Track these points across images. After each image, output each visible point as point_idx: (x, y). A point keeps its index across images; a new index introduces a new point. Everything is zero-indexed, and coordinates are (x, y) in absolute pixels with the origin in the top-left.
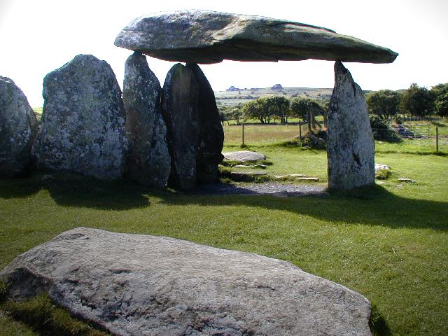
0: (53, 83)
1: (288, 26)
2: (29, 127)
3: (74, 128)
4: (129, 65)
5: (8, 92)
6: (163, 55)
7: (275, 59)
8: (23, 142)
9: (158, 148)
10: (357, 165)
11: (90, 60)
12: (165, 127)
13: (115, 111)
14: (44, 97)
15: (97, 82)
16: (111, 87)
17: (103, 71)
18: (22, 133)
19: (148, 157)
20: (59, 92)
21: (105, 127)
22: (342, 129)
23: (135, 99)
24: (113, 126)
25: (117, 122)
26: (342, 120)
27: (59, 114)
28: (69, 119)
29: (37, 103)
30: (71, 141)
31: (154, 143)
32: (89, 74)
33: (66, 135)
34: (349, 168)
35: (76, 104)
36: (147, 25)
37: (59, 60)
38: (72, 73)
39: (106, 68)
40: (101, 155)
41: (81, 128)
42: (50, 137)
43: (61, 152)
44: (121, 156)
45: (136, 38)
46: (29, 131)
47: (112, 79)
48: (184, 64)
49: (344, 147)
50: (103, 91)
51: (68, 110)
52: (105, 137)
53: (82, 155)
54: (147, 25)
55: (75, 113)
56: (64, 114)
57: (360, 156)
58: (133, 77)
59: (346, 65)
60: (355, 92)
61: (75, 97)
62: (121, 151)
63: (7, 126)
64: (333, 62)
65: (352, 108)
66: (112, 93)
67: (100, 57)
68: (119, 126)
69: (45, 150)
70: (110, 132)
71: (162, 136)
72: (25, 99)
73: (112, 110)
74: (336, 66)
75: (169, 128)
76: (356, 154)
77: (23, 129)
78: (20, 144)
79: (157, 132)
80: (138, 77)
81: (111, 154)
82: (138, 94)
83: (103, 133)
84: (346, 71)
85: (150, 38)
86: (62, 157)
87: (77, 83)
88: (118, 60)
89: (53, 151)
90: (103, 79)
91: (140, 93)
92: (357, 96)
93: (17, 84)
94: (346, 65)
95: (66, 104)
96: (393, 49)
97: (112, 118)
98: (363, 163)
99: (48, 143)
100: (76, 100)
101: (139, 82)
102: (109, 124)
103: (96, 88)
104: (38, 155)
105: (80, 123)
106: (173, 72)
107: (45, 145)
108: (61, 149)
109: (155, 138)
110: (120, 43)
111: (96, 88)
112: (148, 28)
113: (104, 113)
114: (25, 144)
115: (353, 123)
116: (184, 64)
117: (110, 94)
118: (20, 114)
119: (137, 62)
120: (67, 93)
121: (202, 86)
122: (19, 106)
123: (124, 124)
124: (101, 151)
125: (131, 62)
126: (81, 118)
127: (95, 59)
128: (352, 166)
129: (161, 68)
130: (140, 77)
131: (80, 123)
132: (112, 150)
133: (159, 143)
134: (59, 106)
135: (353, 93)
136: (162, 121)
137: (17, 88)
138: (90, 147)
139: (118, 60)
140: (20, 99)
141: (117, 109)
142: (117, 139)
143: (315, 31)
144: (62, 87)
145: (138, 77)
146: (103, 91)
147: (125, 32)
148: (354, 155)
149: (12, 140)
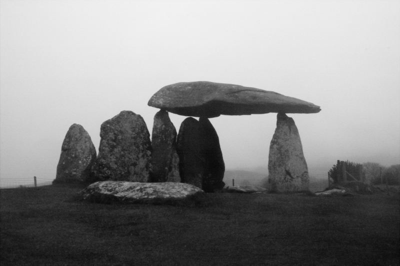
0: (106, 128)
1: (246, 91)
3: (118, 156)
4: (157, 118)
5: (80, 133)
6: (179, 111)
7: (249, 113)
10: (290, 178)
11: (130, 113)
12: (178, 158)
13: (144, 146)
14: (101, 135)
15: (134, 128)
16: (142, 131)
17: (138, 121)
18: (86, 158)
20: (110, 133)
21: (138, 156)
22: (279, 155)
23: (160, 140)
24: (143, 156)
25: (146, 154)
27: (109, 147)
28: (116, 150)
29: (96, 141)
30: (116, 163)
31: (170, 169)
32: (130, 123)
33: (113, 160)
34: (283, 178)
36: (168, 92)
37: (111, 114)
38: (119, 122)
39: (140, 119)
41: (123, 156)
42: (103, 160)
43: (110, 170)
44: (148, 175)
45: (161, 102)
46: (91, 157)
47: (144, 126)
48: (198, 119)
49: (280, 166)
50: (138, 134)
51: (115, 144)
52: (138, 163)
53: (123, 173)
54: (168, 92)
55: (120, 147)
57: (291, 171)
58: (159, 126)
60: (290, 132)
61: (120, 137)
65: (287, 142)
66: (143, 135)
67: (137, 113)
68: (147, 156)
69: (100, 169)
70: (141, 159)
71: (176, 165)
72: (89, 138)
73: (143, 146)
74: (278, 117)
76: (287, 169)
79: (173, 163)
80: (162, 126)
81: (141, 174)
82: (162, 137)
83: (136, 160)
85: (169, 100)
86: (110, 173)
87: (121, 128)
88: (149, 116)
89: (105, 169)
90: (138, 126)
91: (163, 136)
92: (291, 133)
93: (85, 128)
94: (289, 115)
95: (114, 141)
97: (143, 151)
99: (102, 164)
100: (120, 138)
101: (163, 129)
103: (133, 131)
104: (95, 172)
105: (122, 153)
106: (184, 123)
107: (100, 165)
108: (109, 168)
109: (171, 166)
110: (150, 104)
111: (133, 131)
112: (169, 94)
115: (287, 151)
116: (198, 119)
117: (142, 136)
118: (86, 147)
119: (162, 116)
120: (115, 134)
121: (212, 136)
122: (85, 142)
123: (151, 155)
125: (158, 116)
126: (123, 150)
127: (133, 114)
128: (285, 178)
129: (177, 120)
130: (164, 126)
131: (122, 153)
132: (142, 171)
133: (173, 169)
134: (110, 142)
136: (176, 154)
137: (85, 131)
138: (128, 168)
139: (149, 116)
140: (86, 137)
143: (262, 94)
144: (112, 131)
145: (162, 126)
147: (155, 96)
148: (286, 170)
149: (80, 162)
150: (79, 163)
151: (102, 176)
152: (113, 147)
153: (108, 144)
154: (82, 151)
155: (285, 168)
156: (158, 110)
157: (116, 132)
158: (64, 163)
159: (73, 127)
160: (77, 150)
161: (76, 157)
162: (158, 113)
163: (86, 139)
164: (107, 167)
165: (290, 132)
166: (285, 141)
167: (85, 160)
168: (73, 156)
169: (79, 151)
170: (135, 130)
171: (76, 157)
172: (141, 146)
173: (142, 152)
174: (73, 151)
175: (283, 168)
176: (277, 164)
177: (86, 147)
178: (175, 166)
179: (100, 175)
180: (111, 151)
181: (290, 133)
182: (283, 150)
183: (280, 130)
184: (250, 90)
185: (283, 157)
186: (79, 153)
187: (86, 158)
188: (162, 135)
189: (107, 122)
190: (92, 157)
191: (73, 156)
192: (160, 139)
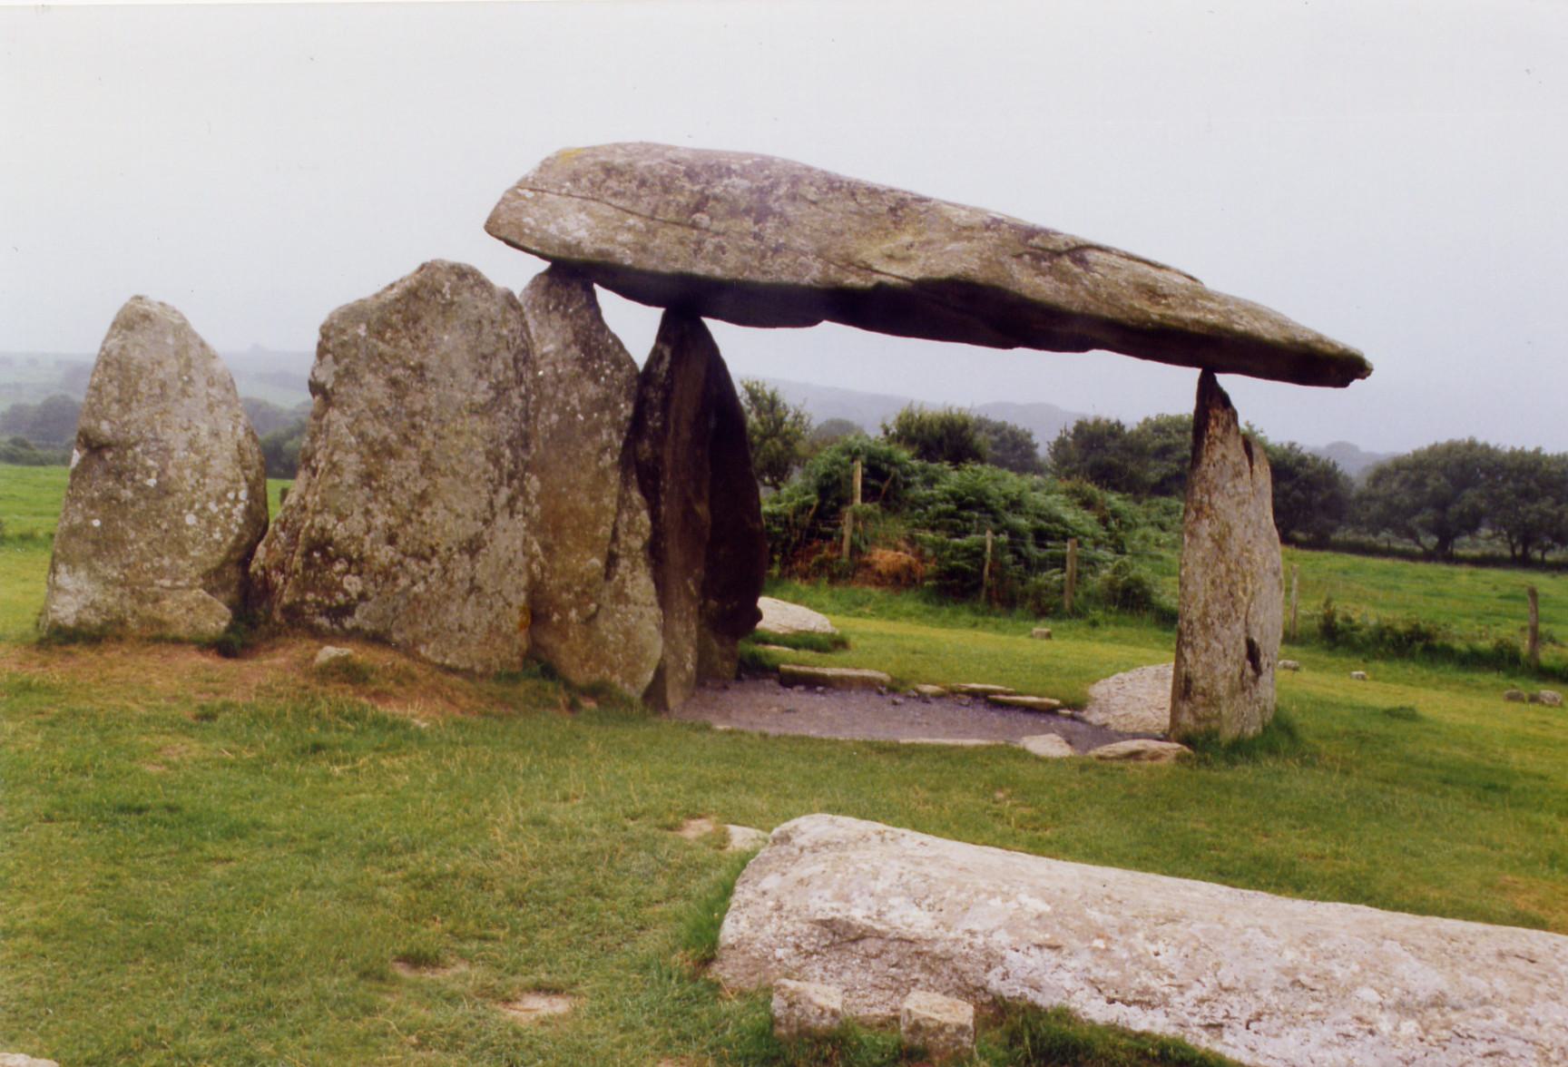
2: (243, 484)
6: (635, 286)
8: (228, 531)
9: (624, 581)
15: (484, 357)
17: (505, 321)
18: (220, 499)
19: (593, 606)
21: (491, 504)
24: (512, 501)
26: (1220, 542)
30: (392, 540)
31: (611, 560)
35: (418, 420)
40: (470, 592)
41: (423, 498)
46: (243, 495)
52: (486, 537)
53: (420, 588)
56: (385, 451)
59: (1226, 381)
60: (1251, 465)
62: (523, 581)
63: (172, 472)
64: (1196, 373)
70: (503, 520)
71: (637, 543)
75: (654, 517)
77: (222, 485)
78: (217, 536)
79: (622, 529)
84: (1225, 401)
89: (339, 567)
92: (1256, 467)
94: (1226, 381)
96: (1369, 357)
97: (511, 476)
98: (1264, 666)
102: (505, 493)
105: (423, 483)
108: (358, 564)
113: (495, 458)
114: (231, 539)
120: (394, 382)
122: (211, 407)
124: (472, 580)
126: (427, 468)
127: (483, 284)
133: (624, 562)
135: (1247, 464)
136: (636, 496)
141: (526, 446)
142: (519, 543)
146: (500, 390)
149: (190, 519)
150: (179, 525)
151: (319, 604)
152: (385, 451)
153: (362, 435)
154: (194, 457)
155: (1247, 631)
156: (545, 265)
157: (399, 372)
158: (96, 523)
159: (134, 320)
160: (167, 451)
161: (164, 491)
162: (541, 275)
163: (213, 391)
164: (350, 561)
165: (1251, 465)
166: (1239, 504)
167: (213, 507)
168: (152, 482)
169: (180, 454)
170: (488, 371)
171: (164, 491)
172: (508, 452)
173: (509, 486)
174: (146, 453)
175: (1238, 628)
176: (1216, 609)
177: (215, 434)
178: (629, 549)
179: (310, 596)
180: (367, 478)
181: (1252, 472)
182: (1234, 546)
183: (1217, 456)
184: (1130, 257)
185: (1238, 577)
186: (180, 468)
187: (220, 499)
188: (567, 394)
189: (354, 313)
190: (249, 497)
191: (152, 482)
192: (561, 411)
